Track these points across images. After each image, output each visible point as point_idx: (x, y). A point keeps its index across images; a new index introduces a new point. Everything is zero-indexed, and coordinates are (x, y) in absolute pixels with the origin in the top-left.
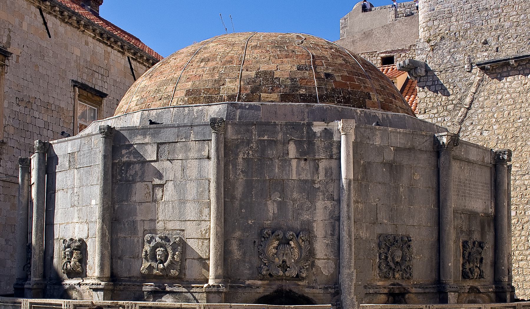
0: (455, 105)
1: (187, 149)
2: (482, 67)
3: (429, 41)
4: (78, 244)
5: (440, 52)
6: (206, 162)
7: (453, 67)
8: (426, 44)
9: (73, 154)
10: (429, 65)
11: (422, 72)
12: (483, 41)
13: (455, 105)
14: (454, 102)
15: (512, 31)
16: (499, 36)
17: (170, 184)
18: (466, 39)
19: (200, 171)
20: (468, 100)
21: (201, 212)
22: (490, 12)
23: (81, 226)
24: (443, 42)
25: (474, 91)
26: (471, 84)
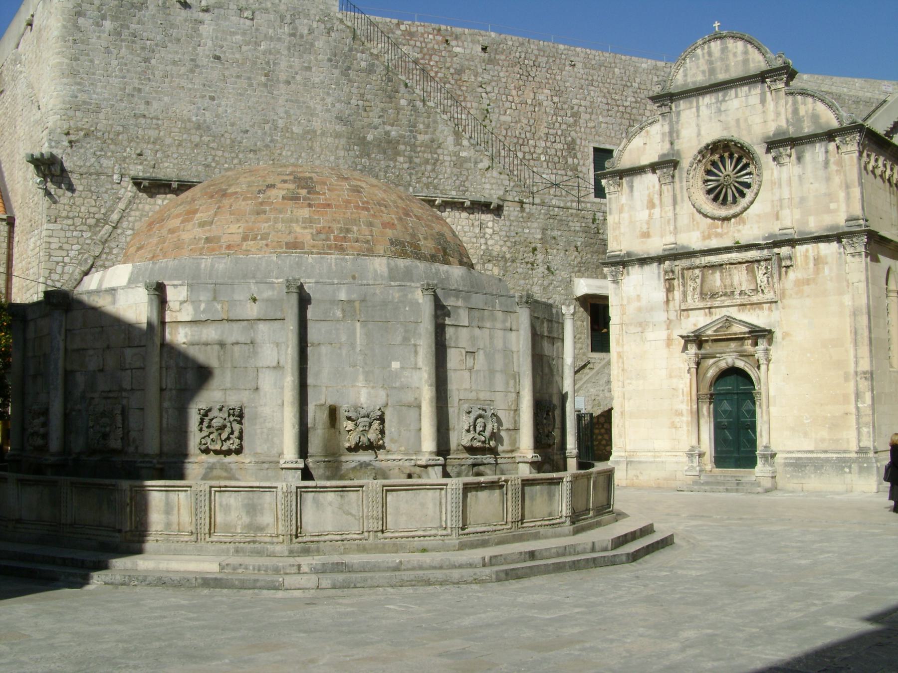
0: (98, 220)
1: (493, 319)
2: (137, 182)
3: (68, 134)
4: (379, 413)
5: (82, 151)
6: (509, 334)
7: (98, 174)
8: (64, 138)
9: (350, 302)
10: (65, 165)
11: (56, 170)
12: (138, 151)
13: (98, 220)
14: (96, 216)
15: (174, 149)
16: (157, 151)
17: (481, 352)
18: (116, 144)
19: (505, 343)
20: (115, 217)
21: (507, 384)
22: (149, 121)
23: (372, 391)
24: (88, 140)
25: (123, 208)
26: (120, 199)
